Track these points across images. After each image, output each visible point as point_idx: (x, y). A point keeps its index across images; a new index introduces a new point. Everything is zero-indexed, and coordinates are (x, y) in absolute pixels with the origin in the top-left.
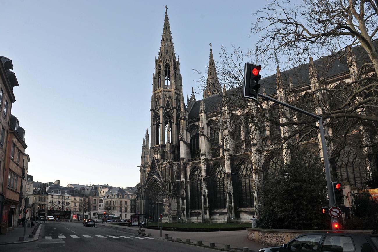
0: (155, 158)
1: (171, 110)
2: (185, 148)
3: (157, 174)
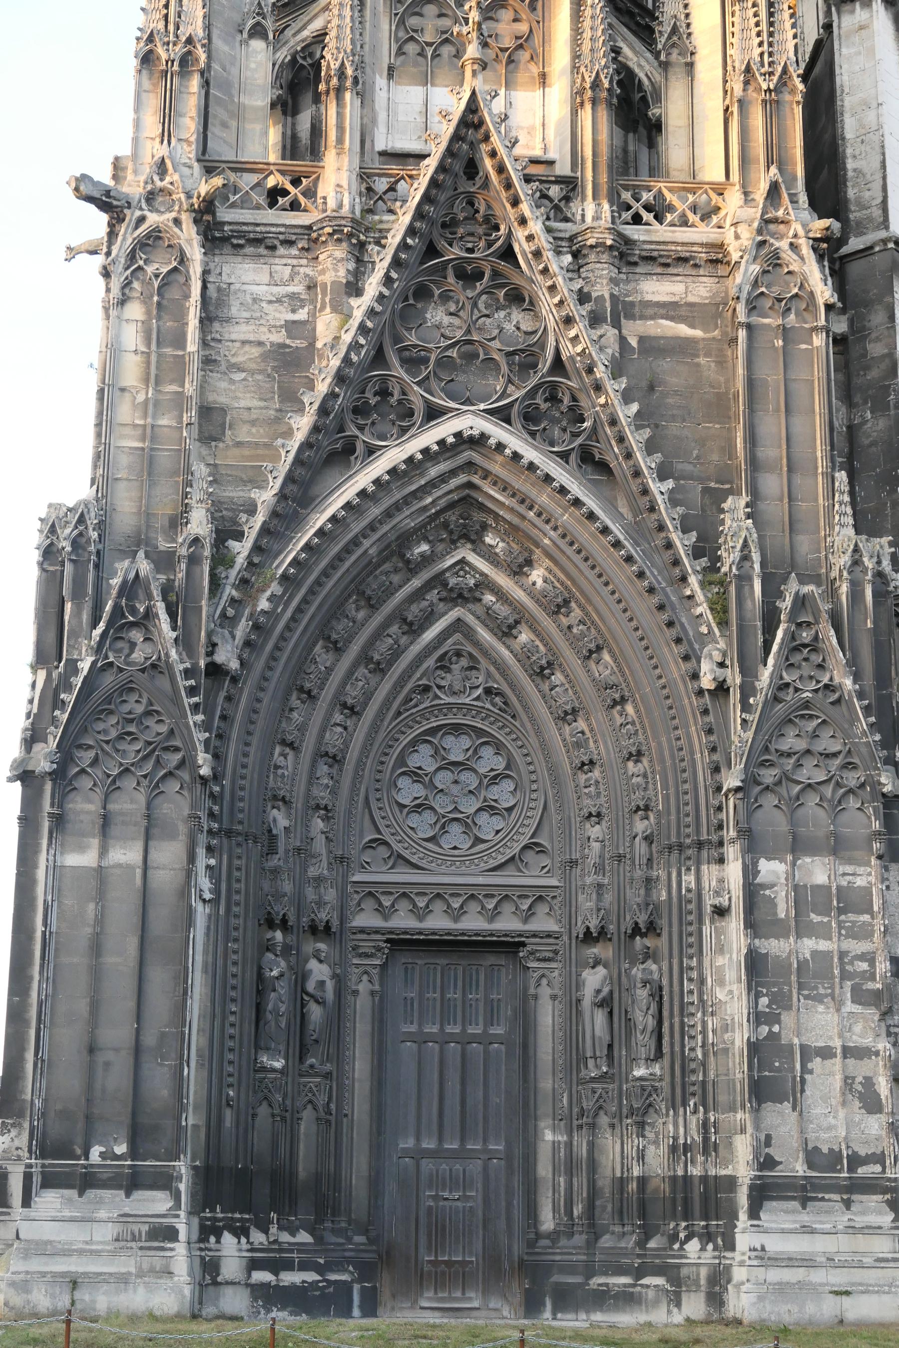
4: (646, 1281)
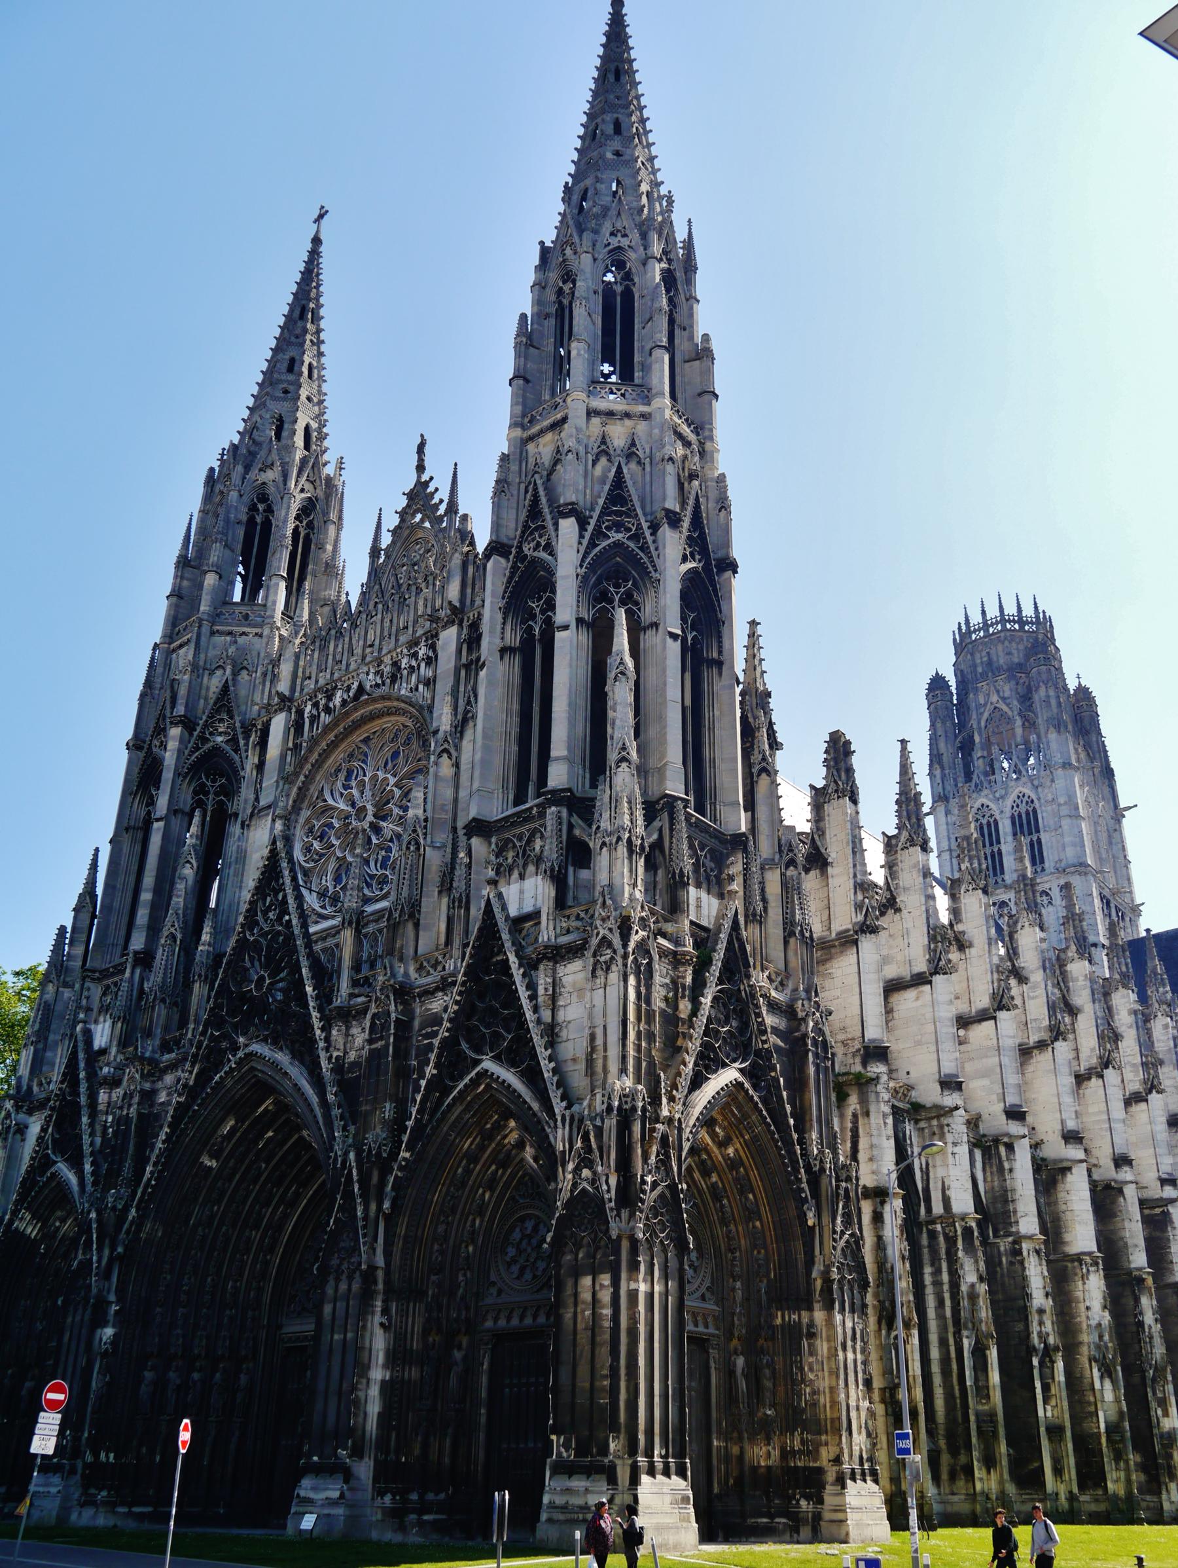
0: (504, 907)
1: (636, 537)
4: (777, 1520)
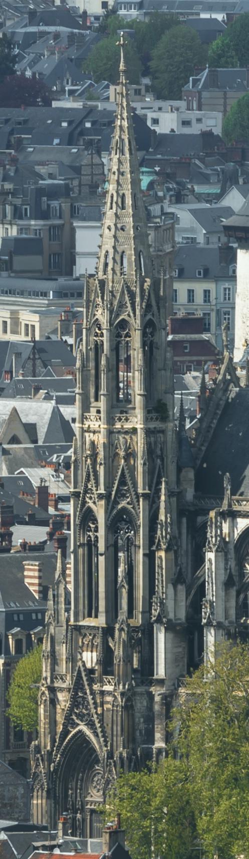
2: (169, 645)
3: (91, 725)
